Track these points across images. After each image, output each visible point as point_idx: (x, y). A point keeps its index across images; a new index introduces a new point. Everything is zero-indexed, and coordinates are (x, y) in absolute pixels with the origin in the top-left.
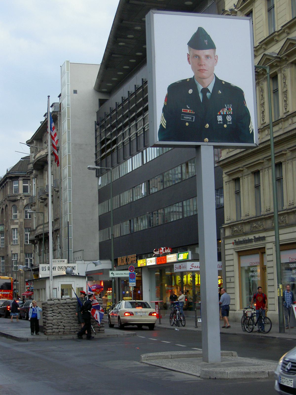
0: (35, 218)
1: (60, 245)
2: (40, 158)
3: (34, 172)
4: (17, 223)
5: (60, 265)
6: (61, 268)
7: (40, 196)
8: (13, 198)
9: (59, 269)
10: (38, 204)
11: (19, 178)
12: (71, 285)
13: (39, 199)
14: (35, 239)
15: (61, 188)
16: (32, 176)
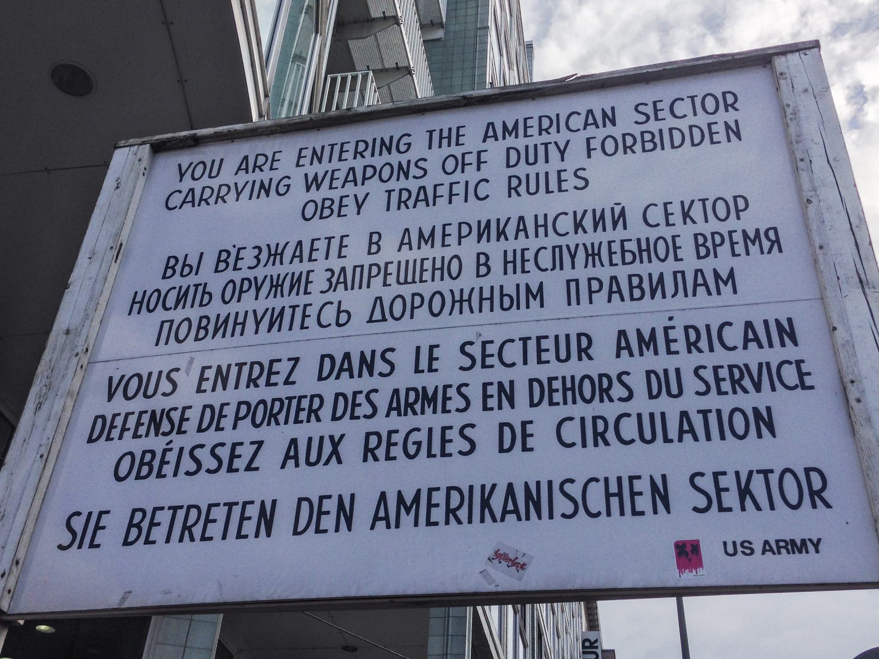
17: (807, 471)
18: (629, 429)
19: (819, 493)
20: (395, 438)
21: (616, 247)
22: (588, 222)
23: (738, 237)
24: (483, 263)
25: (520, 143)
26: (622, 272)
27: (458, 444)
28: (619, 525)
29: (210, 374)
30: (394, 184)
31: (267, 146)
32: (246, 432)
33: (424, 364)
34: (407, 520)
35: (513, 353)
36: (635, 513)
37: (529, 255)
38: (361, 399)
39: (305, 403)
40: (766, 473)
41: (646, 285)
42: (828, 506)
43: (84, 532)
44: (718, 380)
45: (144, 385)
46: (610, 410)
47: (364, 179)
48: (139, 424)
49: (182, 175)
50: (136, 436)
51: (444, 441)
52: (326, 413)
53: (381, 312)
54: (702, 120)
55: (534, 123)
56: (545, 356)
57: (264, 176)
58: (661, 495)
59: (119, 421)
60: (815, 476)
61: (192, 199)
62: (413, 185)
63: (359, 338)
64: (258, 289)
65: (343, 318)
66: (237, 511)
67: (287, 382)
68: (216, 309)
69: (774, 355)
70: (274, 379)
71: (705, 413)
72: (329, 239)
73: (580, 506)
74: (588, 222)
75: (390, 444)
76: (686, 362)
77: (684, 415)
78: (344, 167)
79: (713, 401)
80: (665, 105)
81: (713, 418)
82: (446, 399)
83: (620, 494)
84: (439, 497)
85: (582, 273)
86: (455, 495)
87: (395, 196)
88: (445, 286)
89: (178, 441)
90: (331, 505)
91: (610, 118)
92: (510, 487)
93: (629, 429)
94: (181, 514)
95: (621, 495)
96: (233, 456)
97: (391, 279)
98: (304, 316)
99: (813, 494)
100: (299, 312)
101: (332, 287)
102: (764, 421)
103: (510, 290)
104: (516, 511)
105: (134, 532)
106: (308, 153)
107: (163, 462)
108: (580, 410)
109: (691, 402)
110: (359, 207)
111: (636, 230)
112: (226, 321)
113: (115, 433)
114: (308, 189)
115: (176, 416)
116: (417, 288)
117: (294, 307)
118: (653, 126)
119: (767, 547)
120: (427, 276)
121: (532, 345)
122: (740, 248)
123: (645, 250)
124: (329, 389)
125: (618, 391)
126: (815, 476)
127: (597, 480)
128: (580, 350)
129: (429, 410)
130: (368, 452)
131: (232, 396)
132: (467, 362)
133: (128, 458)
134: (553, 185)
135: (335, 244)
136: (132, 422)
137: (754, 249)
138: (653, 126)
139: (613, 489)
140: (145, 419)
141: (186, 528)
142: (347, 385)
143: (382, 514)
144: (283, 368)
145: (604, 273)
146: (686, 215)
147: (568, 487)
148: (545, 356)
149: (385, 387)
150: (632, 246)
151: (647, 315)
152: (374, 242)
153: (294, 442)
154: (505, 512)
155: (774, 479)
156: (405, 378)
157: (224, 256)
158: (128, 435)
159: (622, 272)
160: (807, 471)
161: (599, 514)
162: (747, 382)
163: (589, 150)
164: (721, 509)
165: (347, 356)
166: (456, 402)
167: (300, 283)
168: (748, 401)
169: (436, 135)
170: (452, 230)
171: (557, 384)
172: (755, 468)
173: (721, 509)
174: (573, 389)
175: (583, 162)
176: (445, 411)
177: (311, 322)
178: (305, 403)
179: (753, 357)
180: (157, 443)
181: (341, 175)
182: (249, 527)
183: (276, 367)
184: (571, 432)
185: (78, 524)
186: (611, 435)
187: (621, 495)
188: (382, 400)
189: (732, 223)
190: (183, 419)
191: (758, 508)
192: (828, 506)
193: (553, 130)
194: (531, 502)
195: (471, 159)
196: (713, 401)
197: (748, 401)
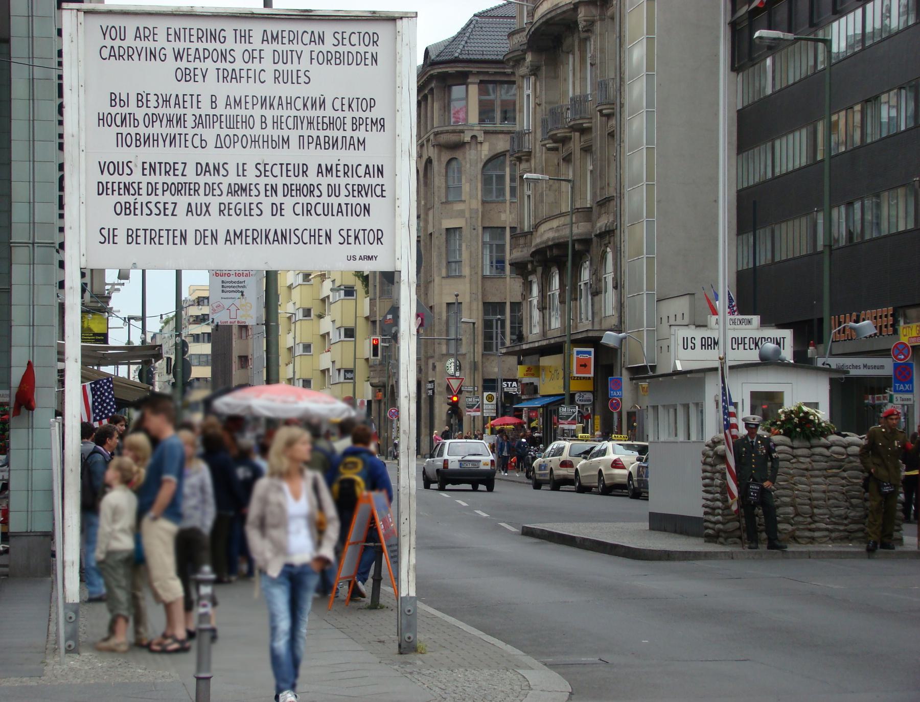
0: (529, 196)
1: (615, 279)
2: (553, 14)
3: (529, 58)
4: (461, 214)
5: (739, 334)
6: (739, 342)
7: (551, 130)
8: (453, 138)
9: (735, 346)
10: (538, 155)
11: (468, 78)
12: (781, 393)
13: (546, 139)
14: (531, 259)
15: (622, 105)
16: (523, 70)
18: (319, 209)
20: (231, 206)
21: (320, 120)
22: (309, 105)
23: (369, 121)
24: (264, 121)
25: (280, 48)
26: (322, 134)
27: (256, 211)
28: (314, 247)
29: (147, 166)
30: (219, 65)
31: (150, 23)
32: (168, 197)
33: (241, 173)
34: (238, 241)
35: (277, 171)
37: (284, 120)
38: (215, 186)
39: (192, 186)
40: (364, 230)
41: (331, 142)
43: (109, 237)
44: (353, 190)
45: (116, 168)
46: (313, 200)
47: (205, 58)
48: (119, 189)
49: (104, 35)
50: (119, 194)
51: (250, 209)
52: (201, 191)
53: (220, 143)
54: (362, 49)
55: (285, 34)
56: (289, 173)
57: (150, 44)
58: (328, 237)
59: (110, 186)
61: (114, 54)
62: (230, 67)
63: (212, 156)
64: (161, 121)
65: (204, 144)
66: (171, 233)
67: (183, 175)
68: (141, 130)
69: (374, 181)
70: (176, 172)
71: (347, 204)
72: (192, 95)
73: (300, 239)
74: (309, 105)
75: (229, 209)
76: (343, 181)
77: (340, 204)
78: (194, 46)
79: (350, 200)
80: (346, 36)
81: (349, 206)
82: (250, 190)
84: (249, 233)
85: (306, 133)
87: (221, 72)
88: (248, 132)
89: (140, 199)
90: (208, 233)
91: (322, 39)
93: (319, 209)
94: (148, 232)
96: (165, 209)
97: (223, 125)
98: (186, 141)
100: (183, 137)
101: (196, 126)
102: (367, 209)
103: (276, 138)
105: (130, 239)
106: (171, 32)
107: (135, 209)
108: (302, 200)
109: (342, 200)
110: (204, 77)
111: (329, 112)
112: (149, 137)
113: (110, 191)
114: (176, 59)
115: (135, 186)
116: (235, 131)
117: (180, 134)
118: (340, 48)
119: (361, 258)
120: (239, 125)
121: (284, 167)
122: (369, 127)
123: (332, 124)
124: (202, 180)
125: (316, 193)
128: (303, 172)
129: (244, 195)
130: (220, 211)
131: (159, 179)
132: (258, 174)
133: (118, 205)
134: (295, 80)
135: (195, 98)
136: (116, 187)
137: (374, 128)
138: (340, 48)
139: (312, 234)
140: (122, 186)
141: (151, 239)
142: (209, 179)
144: (180, 167)
145: (315, 134)
146: (350, 106)
148: (289, 173)
149: (225, 182)
150: (326, 120)
151: (329, 157)
152: (213, 102)
153: (190, 204)
155: (366, 232)
156: (233, 179)
157: (140, 98)
158: (116, 193)
159: (322, 134)
162: (363, 193)
163: (312, 59)
165: (207, 164)
166: (254, 192)
167: (181, 120)
168: (363, 200)
169: (238, 32)
170: (249, 99)
171: (294, 187)
174: (299, 190)
175: (309, 67)
176: (250, 196)
177: (189, 144)
178: (192, 186)
179: (366, 181)
180: (131, 199)
181: (192, 52)
182: (177, 240)
183: (177, 166)
184: (298, 209)
185: (105, 232)
186: (313, 212)
187: (314, 236)
188: (225, 188)
189: (367, 114)
190: (139, 189)
193: (295, 42)
194: (283, 237)
195: (256, 54)
196: (350, 200)
197: (363, 200)
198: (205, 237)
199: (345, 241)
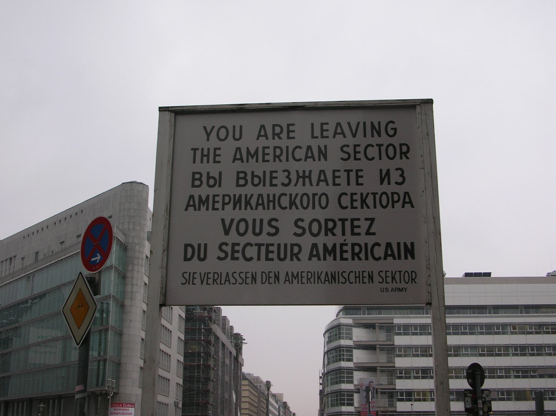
17: (412, 272)
19: (414, 279)
34: (295, 281)
36: (363, 283)
40: (400, 272)
42: (416, 283)
58: (371, 278)
60: (413, 273)
73: (347, 280)
83: (359, 277)
84: (304, 275)
86: (309, 274)
90: (272, 275)
92: (327, 273)
95: (359, 277)
99: (412, 279)
104: (328, 280)
126: (413, 273)
127: (352, 272)
139: (357, 275)
143: (287, 279)
147: (344, 273)
154: (325, 281)
160: (412, 272)
161: (352, 283)
164: (386, 283)
172: (397, 270)
173: (386, 283)
187: (359, 277)
191: (397, 283)
192: (416, 283)
198: (269, 278)
199: (384, 280)
